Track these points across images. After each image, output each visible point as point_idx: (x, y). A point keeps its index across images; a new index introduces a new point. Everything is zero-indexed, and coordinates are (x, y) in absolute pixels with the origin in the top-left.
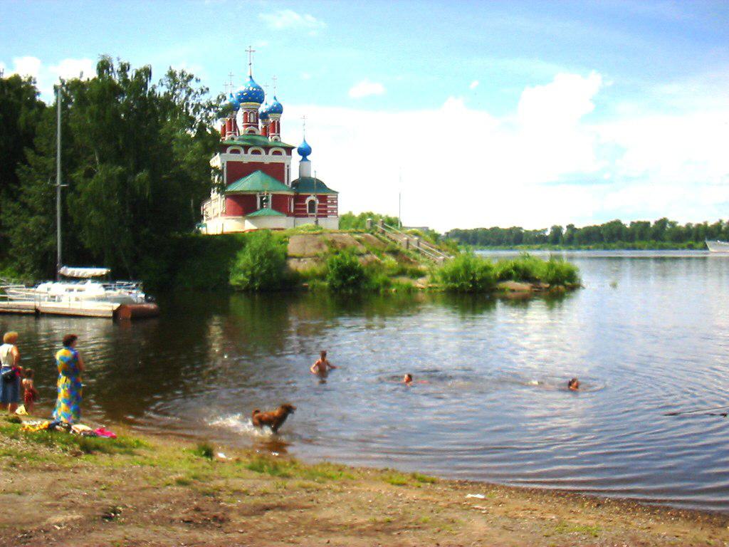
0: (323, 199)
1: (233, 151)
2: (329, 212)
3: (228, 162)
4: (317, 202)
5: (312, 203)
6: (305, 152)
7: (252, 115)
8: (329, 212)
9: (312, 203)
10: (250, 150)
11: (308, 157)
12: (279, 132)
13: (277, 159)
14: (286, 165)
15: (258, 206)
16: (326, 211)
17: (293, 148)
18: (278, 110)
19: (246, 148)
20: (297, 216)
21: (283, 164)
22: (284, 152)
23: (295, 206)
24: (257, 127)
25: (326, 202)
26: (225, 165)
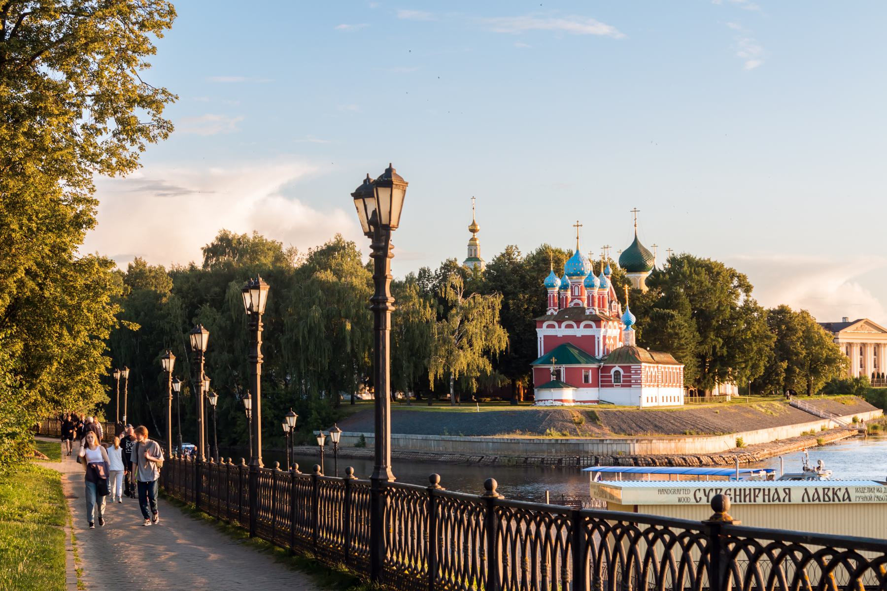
0: (627, 369)
4: (622, 372)
7: (576, 288)
9: (617, 372)
13: (588, 332)
16: (630, 381)
21: (594, 337)
23: (602, 377)
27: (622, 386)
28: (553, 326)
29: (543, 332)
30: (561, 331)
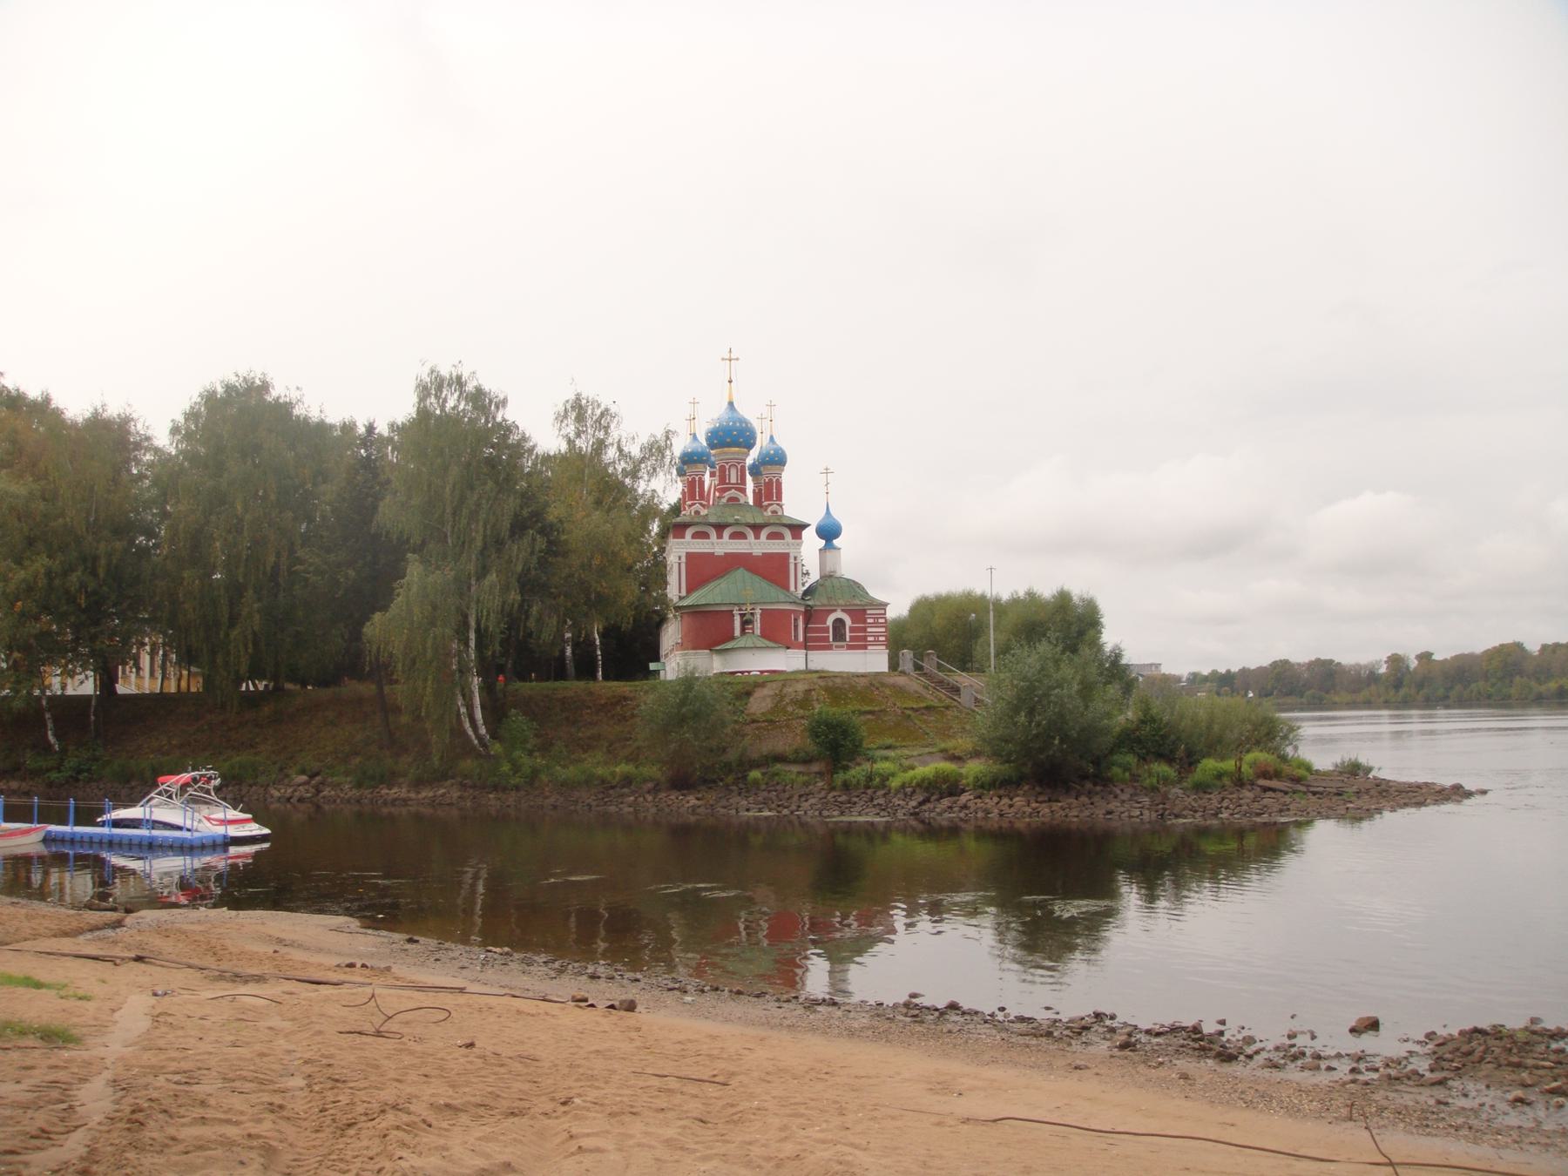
0: (859, 614)
1: (695, 536)
5: (839, 623)
6: (829, 533)
9: (839, 623)
10: (726, 533)
11: (836, 542)
12: (779, 498)
13: (775, 547)
14: (792, 560)
15: (737, 632)
17: (805, 526)
18: (776, 460)
19: (720, 528)
20: (806, 648)
21: (786, 556)
22: (787, 533)
24: (743, 491)
25: (865, 621)
27: (850, 647)
28: (705, 535)
30: (721, 546)
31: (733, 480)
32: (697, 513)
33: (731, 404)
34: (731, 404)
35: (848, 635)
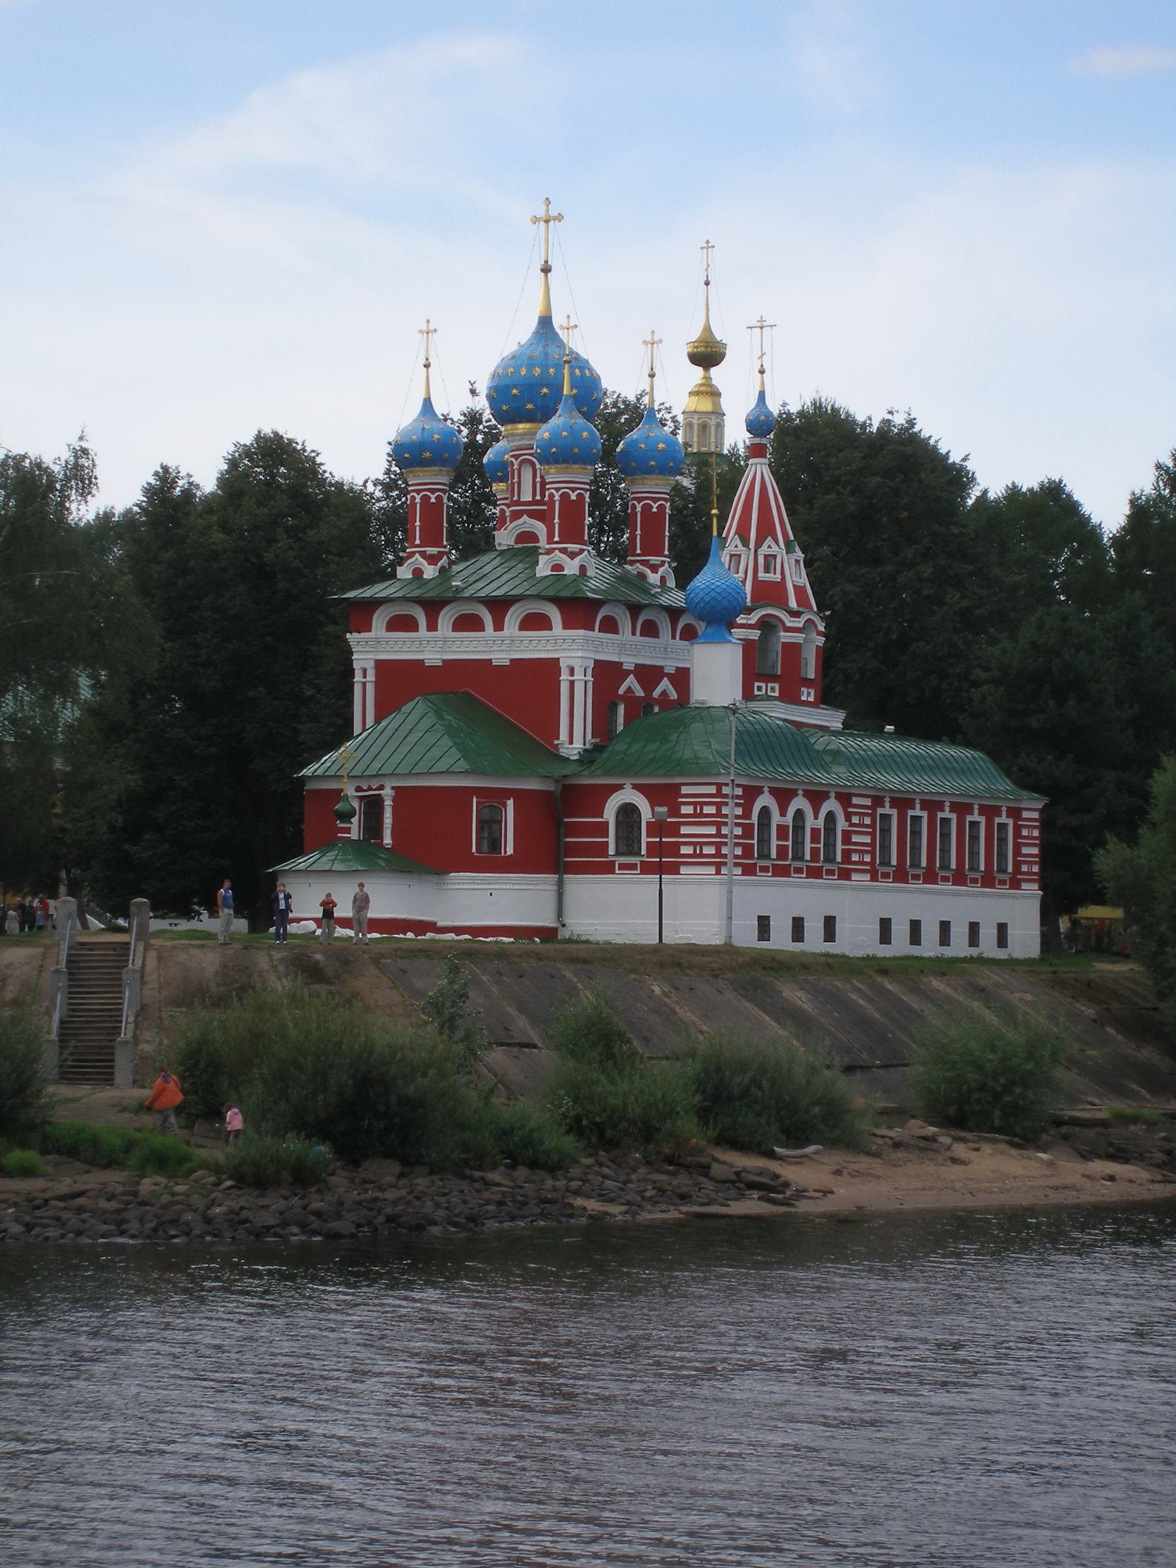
2: (684, 850)
3: (380, 665)
5: (628, 813)
8: (684, 850)
9: (628, 813)
13: (533, 647)
14: (564, 676)
16: (674, 849)
21: (555, 662)
26: (371, 676)
27: (647, 869)
28: (408, 624)
29: (371, 649)
31: (527, 496)
32: (418, 573)
33: (546, 322)
34: (546, 322)
35: (644, 839)
